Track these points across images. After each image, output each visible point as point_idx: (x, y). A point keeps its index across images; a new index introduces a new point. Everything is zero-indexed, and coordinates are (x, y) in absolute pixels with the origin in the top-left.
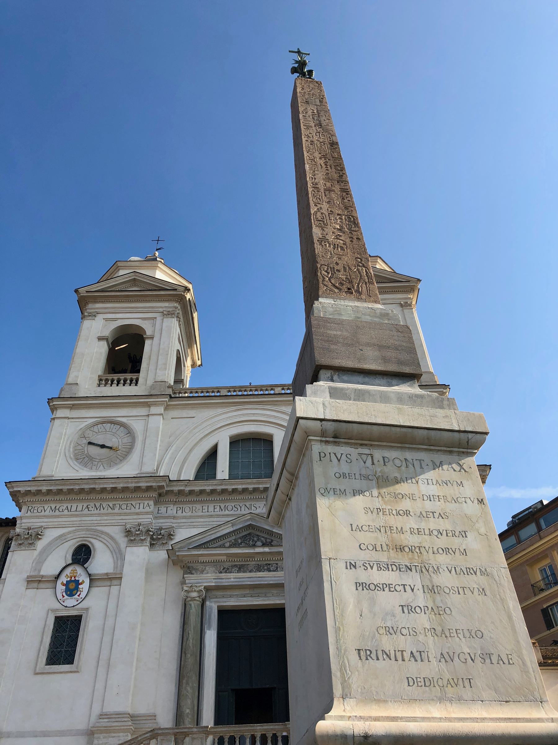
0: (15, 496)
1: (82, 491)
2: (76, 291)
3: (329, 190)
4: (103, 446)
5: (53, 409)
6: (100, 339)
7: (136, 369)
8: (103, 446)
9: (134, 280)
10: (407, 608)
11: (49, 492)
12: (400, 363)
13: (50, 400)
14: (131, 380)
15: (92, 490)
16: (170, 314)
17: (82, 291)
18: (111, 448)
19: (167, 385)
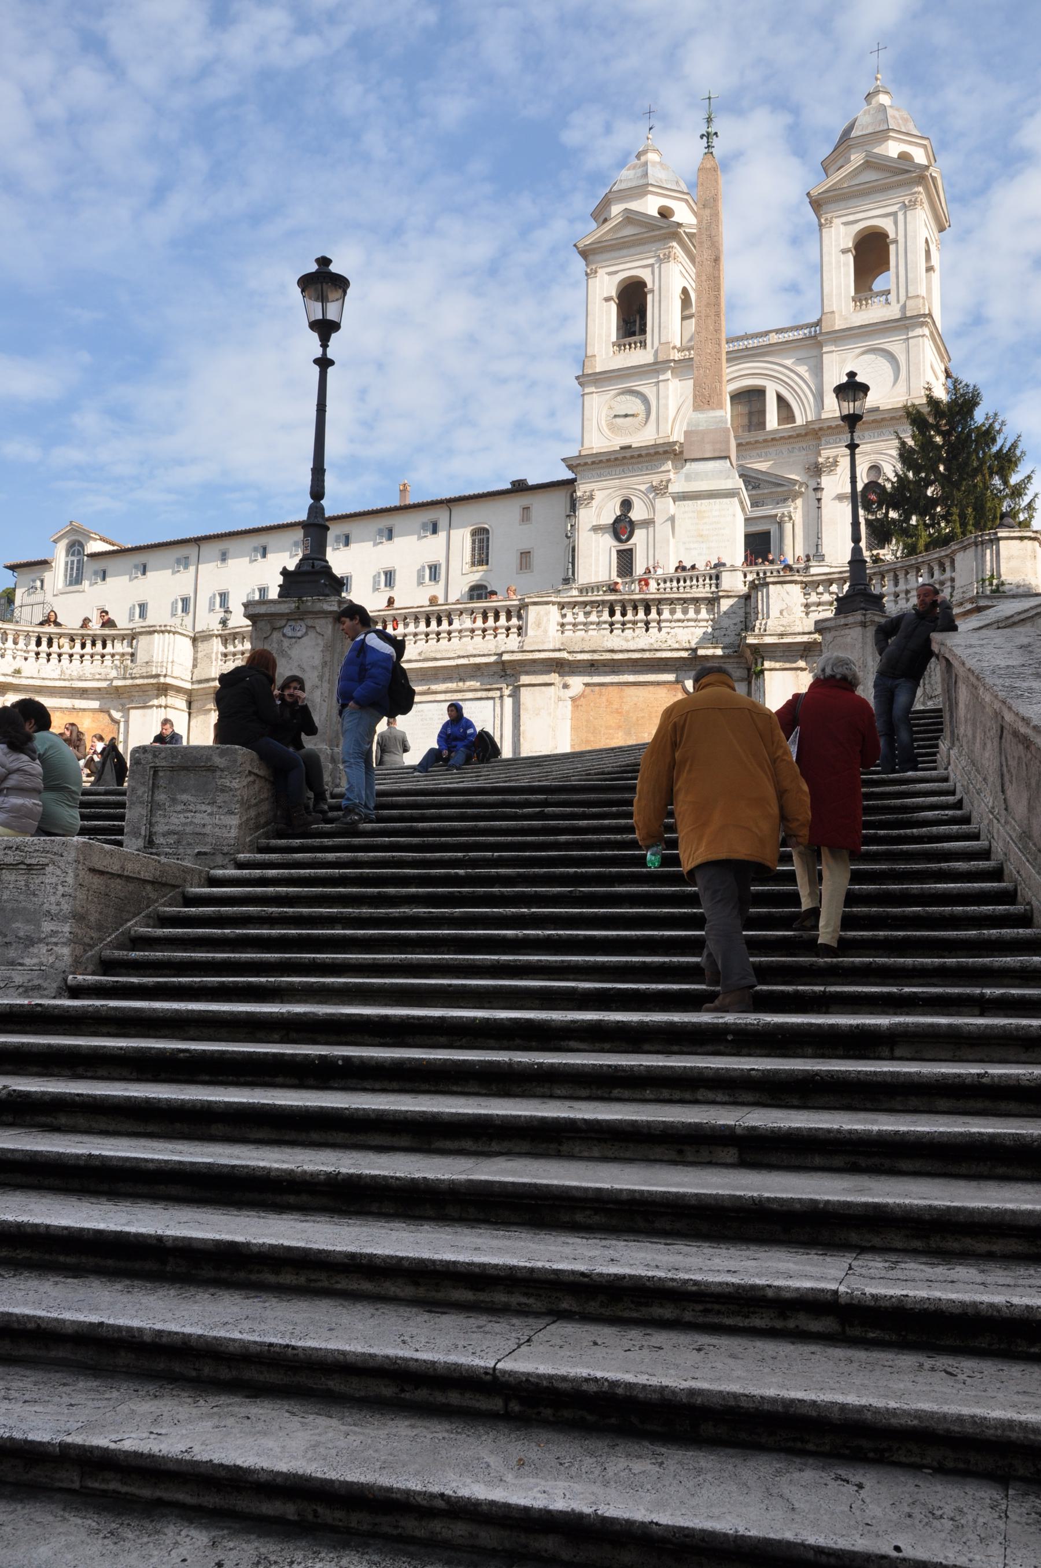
0: (570, 467)
1: (616, 459)
2: (575, 245)
3: (707, 316)
4: (626, 416)
5: (581, 384)
6: (608, 299)
7: (643, 331)
8: (626, 416)
9: (628, 217)
10: (700, 554)
11: (593, 463)
12: (722, 451)
13: (577, 378)
14: (641, 343)
15: (624, 458)
16: (667, 257)
17: (581, 245)
18: (633, 415)
19: (672, 345)
